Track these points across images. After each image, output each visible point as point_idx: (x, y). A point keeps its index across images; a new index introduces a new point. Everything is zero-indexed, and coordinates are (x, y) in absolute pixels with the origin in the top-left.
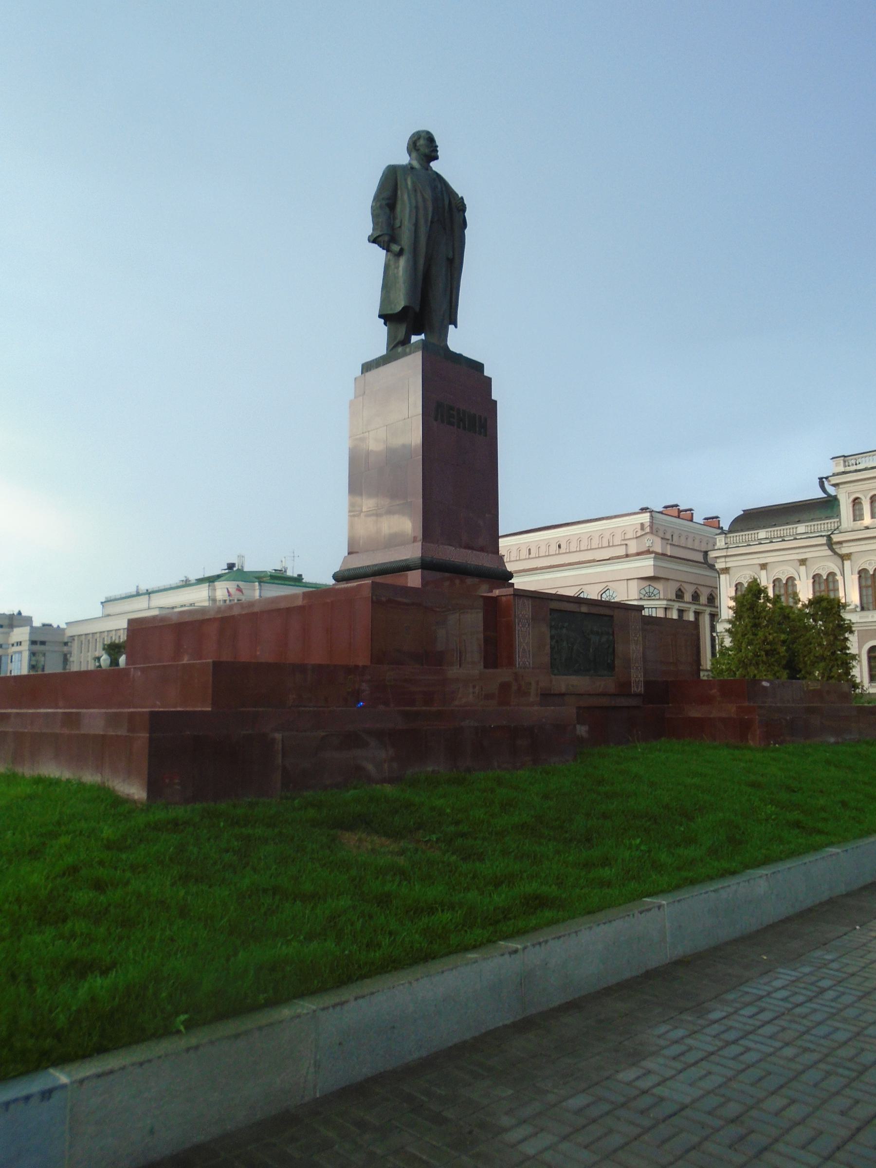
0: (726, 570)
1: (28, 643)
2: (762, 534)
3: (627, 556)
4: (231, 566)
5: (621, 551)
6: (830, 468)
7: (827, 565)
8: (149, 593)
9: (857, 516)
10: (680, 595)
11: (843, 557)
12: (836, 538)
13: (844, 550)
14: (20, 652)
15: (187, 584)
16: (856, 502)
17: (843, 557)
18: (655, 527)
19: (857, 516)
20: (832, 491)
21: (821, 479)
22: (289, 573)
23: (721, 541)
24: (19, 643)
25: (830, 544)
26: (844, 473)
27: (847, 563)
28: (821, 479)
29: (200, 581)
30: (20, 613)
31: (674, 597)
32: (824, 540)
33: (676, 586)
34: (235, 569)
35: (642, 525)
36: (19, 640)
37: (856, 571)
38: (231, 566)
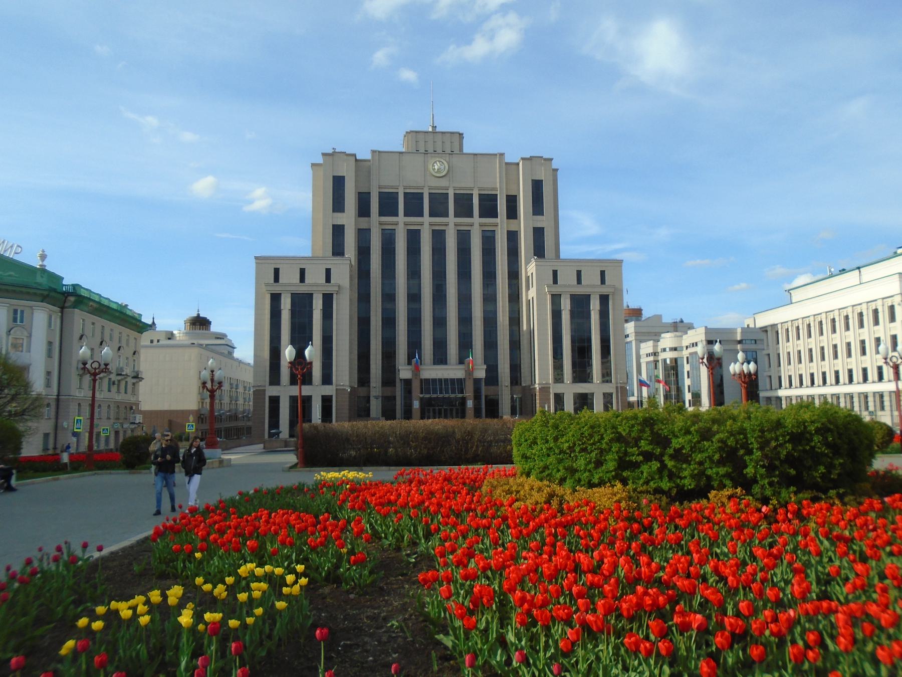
1: (704, 343)
30: (682, 321)
36: (694, 341)
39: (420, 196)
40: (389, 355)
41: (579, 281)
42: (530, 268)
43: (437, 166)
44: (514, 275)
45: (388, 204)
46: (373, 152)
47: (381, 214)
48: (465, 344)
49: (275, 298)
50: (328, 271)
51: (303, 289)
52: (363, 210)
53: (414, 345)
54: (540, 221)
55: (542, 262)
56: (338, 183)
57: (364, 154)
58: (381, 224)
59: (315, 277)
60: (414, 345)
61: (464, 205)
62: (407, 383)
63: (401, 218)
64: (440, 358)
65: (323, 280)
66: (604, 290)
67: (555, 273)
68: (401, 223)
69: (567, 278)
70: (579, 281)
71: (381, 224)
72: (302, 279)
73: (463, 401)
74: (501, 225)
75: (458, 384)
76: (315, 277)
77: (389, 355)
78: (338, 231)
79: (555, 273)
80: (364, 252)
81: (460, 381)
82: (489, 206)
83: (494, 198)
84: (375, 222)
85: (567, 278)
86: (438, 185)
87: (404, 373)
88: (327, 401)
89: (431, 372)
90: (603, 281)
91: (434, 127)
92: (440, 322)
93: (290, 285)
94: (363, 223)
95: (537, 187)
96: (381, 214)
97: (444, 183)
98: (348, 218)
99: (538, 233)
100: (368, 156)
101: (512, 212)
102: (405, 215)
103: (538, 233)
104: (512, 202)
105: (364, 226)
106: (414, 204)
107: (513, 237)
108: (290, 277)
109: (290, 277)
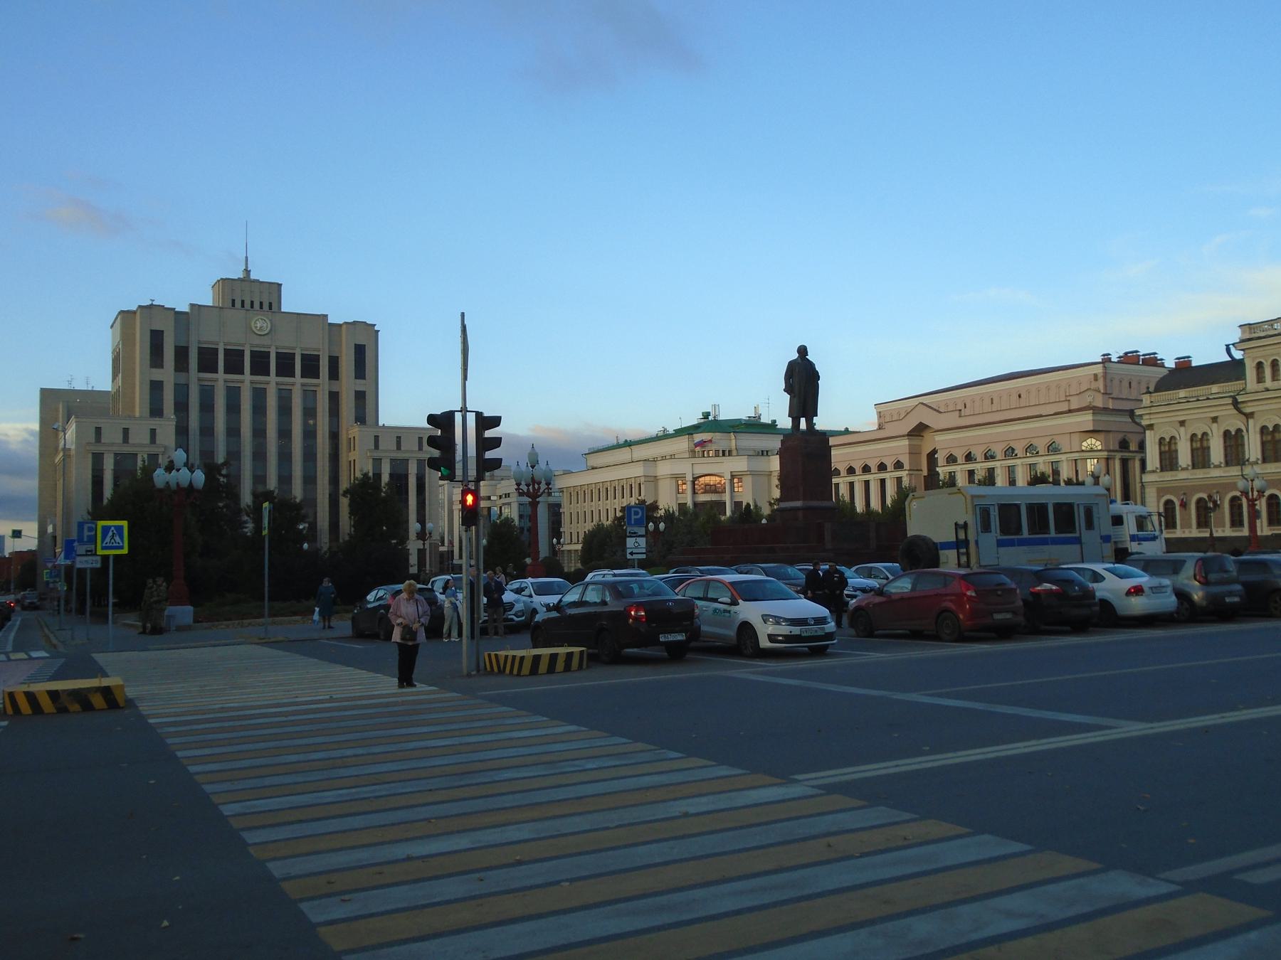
0: (1151, 427)
2: (1182, 393)
3: (1070, 411)
4: (706, 415)
5: (1065, 407)
6: (1236, 336)
7: (1234, 422)
8: (629, 444)
9: (1260, 379)
10: (1124, 445)
11: (1249, 416)
12: (1240, 399)
13: (1248, 410)
14: (509, 504)
15: (664, 436)
16: (1260, 366)
17: (1249, 416)
18: (1109, 377)
19: (1260, 379)
20: (1238, 355)
21: (1227, 346)
22: (765, 419)
23: (1146, 400)
24: (507, 495)
25: (1236, 404)
26: (1249, 340)
27: (1251, 421)
28: (1227, 346)
29: (680, 432)
31: (1117, 447)
32: (1230, 401)
33: (1120, 436)
34: (711, 418)
35: (1096, 376)
37: (1258, 429)
38: (706, 415)
39: (241, 353)
41: (399, 447)
42: (349, 429)
43: (260, 323)
44: (334, 436)
45: (208, 361)
46: (192, 306)
49: (98, 459)
50: (153, 432)
54: (360, 385)
55: (364, 428)
56: (156, 339)
57: (184, 307)
58: (199, 380)
59: (140, 437)
61: (285, 365)
63: (221, 375)
65: (147, 440)
67: (377, 438)
68: (220, 378)
69: (387, 444)
70: (399, 447)
71: (199, 380)
74: (323, 384)
76: (140, 437)
78: (156, 387)
80: (181, 407)
82: (311, 365)
83: (316, 358)
85: (387, 444)
86: (260, 344)
91: (247, 272)
93: (113, 444)
94: (182, 378)
95: (360, 351)
97: (266, 341)
98: (167, 374)
99: (360, 396)
100: (186, 309)
101: (334, 374)
102: (226, 372)
103: (360, 396)
104: (334, 363)
105: (183, 381)
106: (234, 362)
107: (334, 397)
108: (112, 436)
109: (112, 436)
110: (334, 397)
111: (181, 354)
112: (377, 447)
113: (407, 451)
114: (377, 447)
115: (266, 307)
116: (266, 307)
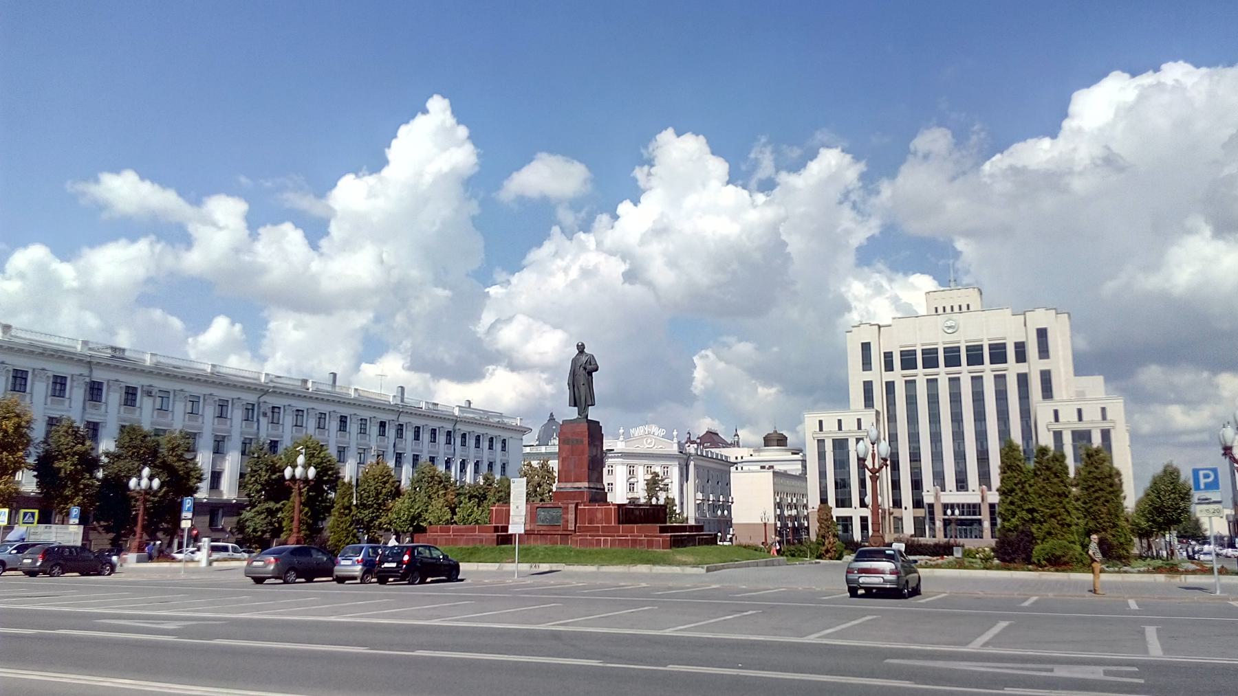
40: (917, 485)
45: (908, 360)
47: (903, 369)
48: (984, 477)
51: (840, 435)
52: (889, 366)
53: (939, 477)
59: (850, 425)
60: (939, 477)
62: (931, 506)
64: (962, 484)
66: (1105, 425)
67: (1056, 412)
72: (840, 428)
73: (980, 522)
74: (1012, 369)
75: (974, 508)
77: (917, 485)
79: (1056, 412)
81: (974, 505)
84: (898, 376)
87: (928, 499)
88: (864, 520)
89: (952, 496)
90: (1104, 418)
92: (960, 456)
93: (831, 432)
94: (888, 376)
96: (903, 369)
101: (1021, 356)
107: (1023, 380)
110: (1023, 380)
111: (888, 357)
112: (1057, 419)
113: (1088, 422)
114: (1057, 419)
115: (964, 308)
116: (964, 308)
